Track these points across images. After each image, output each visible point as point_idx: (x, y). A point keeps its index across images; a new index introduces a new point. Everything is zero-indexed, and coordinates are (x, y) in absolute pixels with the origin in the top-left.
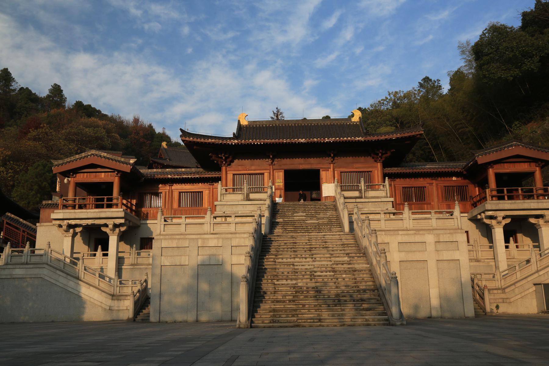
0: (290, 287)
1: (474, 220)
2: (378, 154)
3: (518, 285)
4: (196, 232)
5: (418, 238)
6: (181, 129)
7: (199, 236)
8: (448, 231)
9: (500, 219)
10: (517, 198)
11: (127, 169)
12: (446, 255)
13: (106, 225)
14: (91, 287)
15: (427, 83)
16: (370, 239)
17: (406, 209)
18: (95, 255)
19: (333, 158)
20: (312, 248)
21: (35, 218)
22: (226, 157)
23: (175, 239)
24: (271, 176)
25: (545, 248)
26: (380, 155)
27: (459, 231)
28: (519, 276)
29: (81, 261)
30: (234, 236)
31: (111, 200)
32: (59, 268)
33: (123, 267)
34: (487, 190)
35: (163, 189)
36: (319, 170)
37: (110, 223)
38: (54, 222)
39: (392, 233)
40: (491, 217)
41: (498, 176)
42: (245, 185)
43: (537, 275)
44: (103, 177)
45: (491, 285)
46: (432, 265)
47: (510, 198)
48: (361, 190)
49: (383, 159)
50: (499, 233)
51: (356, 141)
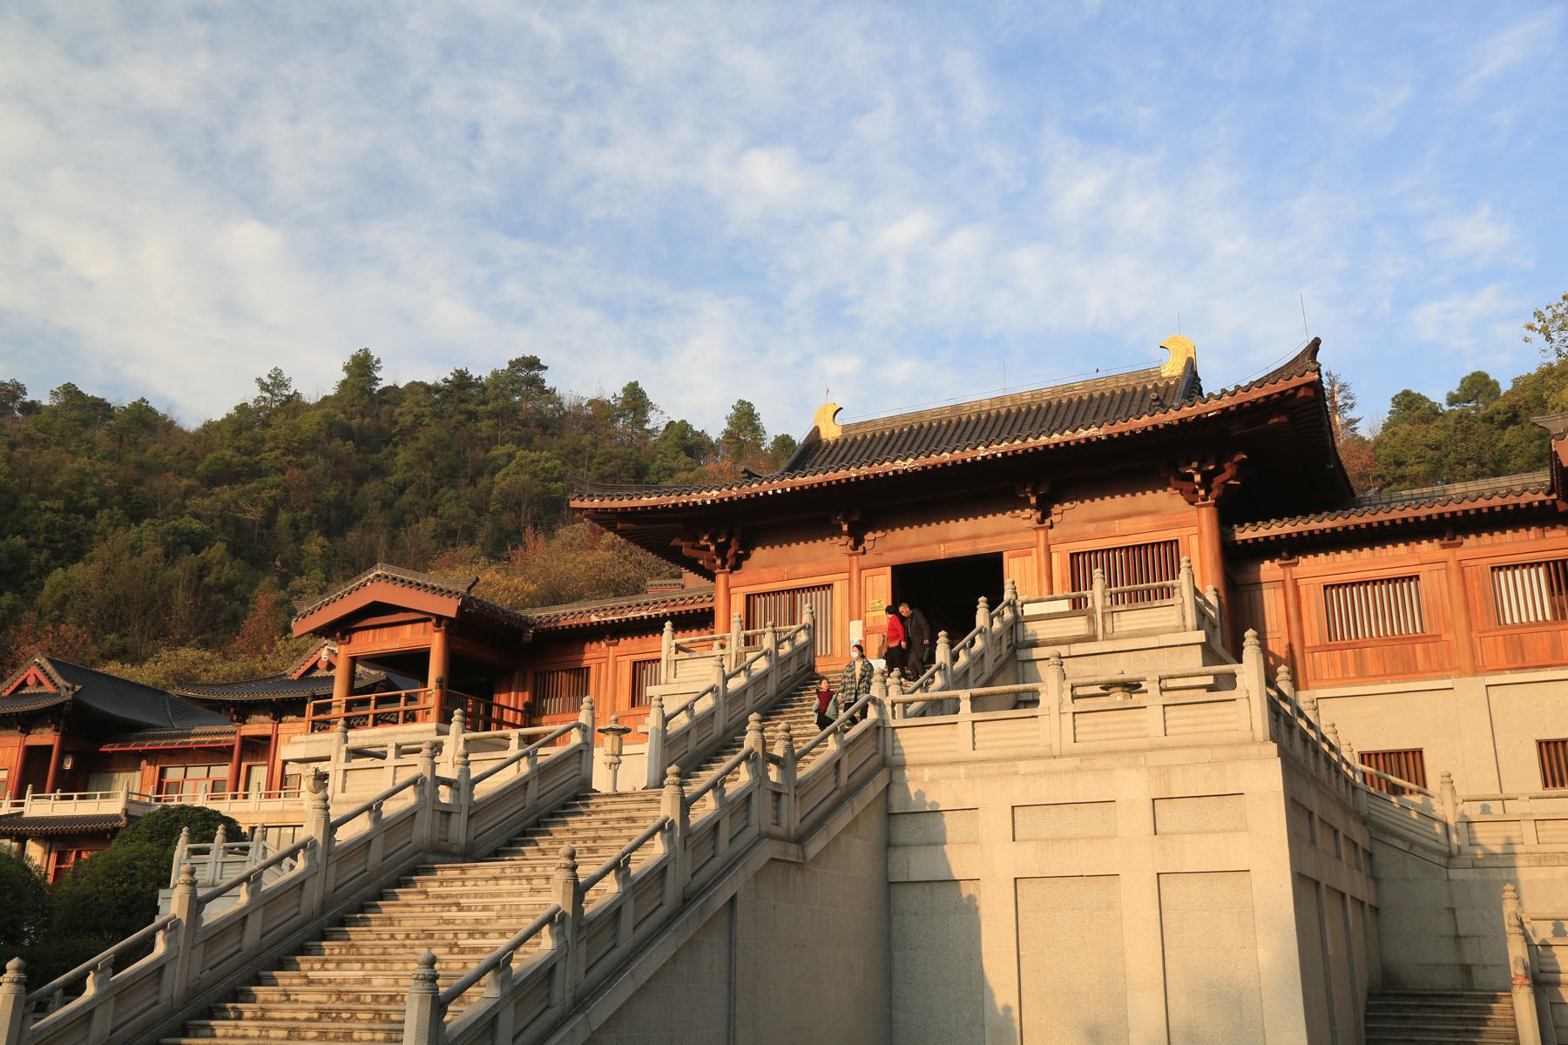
0: (330, 993)
2: (1191, 477)
5: (1086, 787)
8: (1208, 754)
11: (449, 608)
12: (1195, 853)
19: (1045, 510)
22: (718, 546)
24: (855, 591)
26: (1197, 478)
27: (1253, 750)
35: (596, 655)
36: (1000, 555)
39: (992, 768)
48: (1094, 610)
49: (1215, 492)
51: (1078, 442)
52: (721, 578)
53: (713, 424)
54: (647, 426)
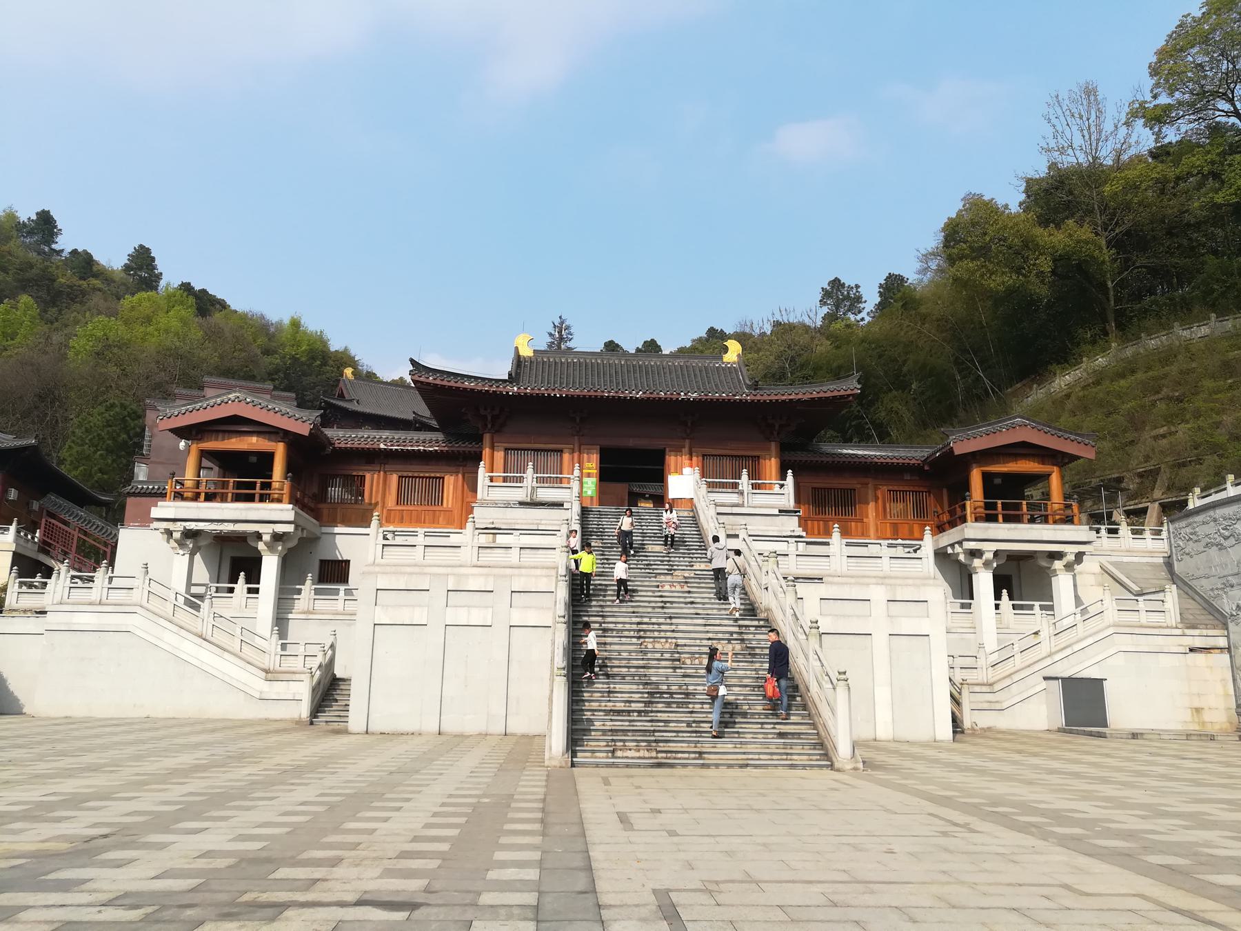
1: (941, 556)
3: (1016, 677)
4: (444, 563)
6: (413, 361)
7: (449, 570)
8: (910, 582)
9: (989, 556)
10: (1016, 519)
11: (304, 429)
12: (906, 626)
13: (259, 536)
14: (226, 655)
15: (839, 295)
16: (781, 595)
17: (836, 535)
18: (231, 590)
20: (665, 602)
21: (116, 516)
23: (405, 573)
25: (1064, 614)
27: (931, 582)
28: (1018, 661)
29: (207, 601)
30: (516, 571)
31: (267, 486)
32: (163, 614)
33: (290, 616)
34: (968, 503)
37: (266, 530)
38: (156, 525)
40: (975, 554)
41: (987, 477)
42: (530, 470)
43: (1049, 661)
44: (253, 443)
45: (971, 676)
46: (880, 641)
47: (1008, 519)
50: (984, 582)
52: (487, 438)
53: (113, 257)
54: (53, 246)
